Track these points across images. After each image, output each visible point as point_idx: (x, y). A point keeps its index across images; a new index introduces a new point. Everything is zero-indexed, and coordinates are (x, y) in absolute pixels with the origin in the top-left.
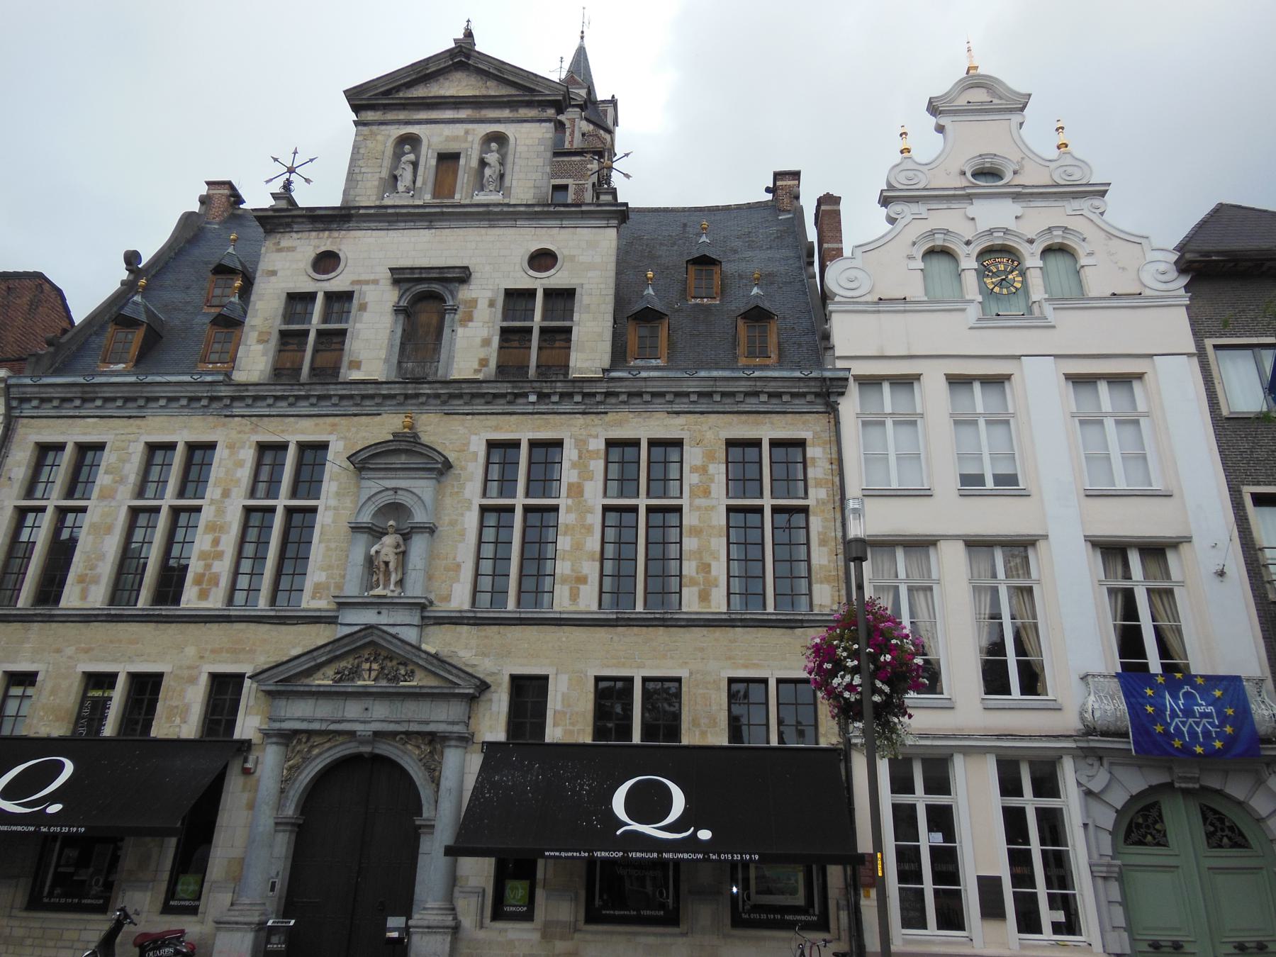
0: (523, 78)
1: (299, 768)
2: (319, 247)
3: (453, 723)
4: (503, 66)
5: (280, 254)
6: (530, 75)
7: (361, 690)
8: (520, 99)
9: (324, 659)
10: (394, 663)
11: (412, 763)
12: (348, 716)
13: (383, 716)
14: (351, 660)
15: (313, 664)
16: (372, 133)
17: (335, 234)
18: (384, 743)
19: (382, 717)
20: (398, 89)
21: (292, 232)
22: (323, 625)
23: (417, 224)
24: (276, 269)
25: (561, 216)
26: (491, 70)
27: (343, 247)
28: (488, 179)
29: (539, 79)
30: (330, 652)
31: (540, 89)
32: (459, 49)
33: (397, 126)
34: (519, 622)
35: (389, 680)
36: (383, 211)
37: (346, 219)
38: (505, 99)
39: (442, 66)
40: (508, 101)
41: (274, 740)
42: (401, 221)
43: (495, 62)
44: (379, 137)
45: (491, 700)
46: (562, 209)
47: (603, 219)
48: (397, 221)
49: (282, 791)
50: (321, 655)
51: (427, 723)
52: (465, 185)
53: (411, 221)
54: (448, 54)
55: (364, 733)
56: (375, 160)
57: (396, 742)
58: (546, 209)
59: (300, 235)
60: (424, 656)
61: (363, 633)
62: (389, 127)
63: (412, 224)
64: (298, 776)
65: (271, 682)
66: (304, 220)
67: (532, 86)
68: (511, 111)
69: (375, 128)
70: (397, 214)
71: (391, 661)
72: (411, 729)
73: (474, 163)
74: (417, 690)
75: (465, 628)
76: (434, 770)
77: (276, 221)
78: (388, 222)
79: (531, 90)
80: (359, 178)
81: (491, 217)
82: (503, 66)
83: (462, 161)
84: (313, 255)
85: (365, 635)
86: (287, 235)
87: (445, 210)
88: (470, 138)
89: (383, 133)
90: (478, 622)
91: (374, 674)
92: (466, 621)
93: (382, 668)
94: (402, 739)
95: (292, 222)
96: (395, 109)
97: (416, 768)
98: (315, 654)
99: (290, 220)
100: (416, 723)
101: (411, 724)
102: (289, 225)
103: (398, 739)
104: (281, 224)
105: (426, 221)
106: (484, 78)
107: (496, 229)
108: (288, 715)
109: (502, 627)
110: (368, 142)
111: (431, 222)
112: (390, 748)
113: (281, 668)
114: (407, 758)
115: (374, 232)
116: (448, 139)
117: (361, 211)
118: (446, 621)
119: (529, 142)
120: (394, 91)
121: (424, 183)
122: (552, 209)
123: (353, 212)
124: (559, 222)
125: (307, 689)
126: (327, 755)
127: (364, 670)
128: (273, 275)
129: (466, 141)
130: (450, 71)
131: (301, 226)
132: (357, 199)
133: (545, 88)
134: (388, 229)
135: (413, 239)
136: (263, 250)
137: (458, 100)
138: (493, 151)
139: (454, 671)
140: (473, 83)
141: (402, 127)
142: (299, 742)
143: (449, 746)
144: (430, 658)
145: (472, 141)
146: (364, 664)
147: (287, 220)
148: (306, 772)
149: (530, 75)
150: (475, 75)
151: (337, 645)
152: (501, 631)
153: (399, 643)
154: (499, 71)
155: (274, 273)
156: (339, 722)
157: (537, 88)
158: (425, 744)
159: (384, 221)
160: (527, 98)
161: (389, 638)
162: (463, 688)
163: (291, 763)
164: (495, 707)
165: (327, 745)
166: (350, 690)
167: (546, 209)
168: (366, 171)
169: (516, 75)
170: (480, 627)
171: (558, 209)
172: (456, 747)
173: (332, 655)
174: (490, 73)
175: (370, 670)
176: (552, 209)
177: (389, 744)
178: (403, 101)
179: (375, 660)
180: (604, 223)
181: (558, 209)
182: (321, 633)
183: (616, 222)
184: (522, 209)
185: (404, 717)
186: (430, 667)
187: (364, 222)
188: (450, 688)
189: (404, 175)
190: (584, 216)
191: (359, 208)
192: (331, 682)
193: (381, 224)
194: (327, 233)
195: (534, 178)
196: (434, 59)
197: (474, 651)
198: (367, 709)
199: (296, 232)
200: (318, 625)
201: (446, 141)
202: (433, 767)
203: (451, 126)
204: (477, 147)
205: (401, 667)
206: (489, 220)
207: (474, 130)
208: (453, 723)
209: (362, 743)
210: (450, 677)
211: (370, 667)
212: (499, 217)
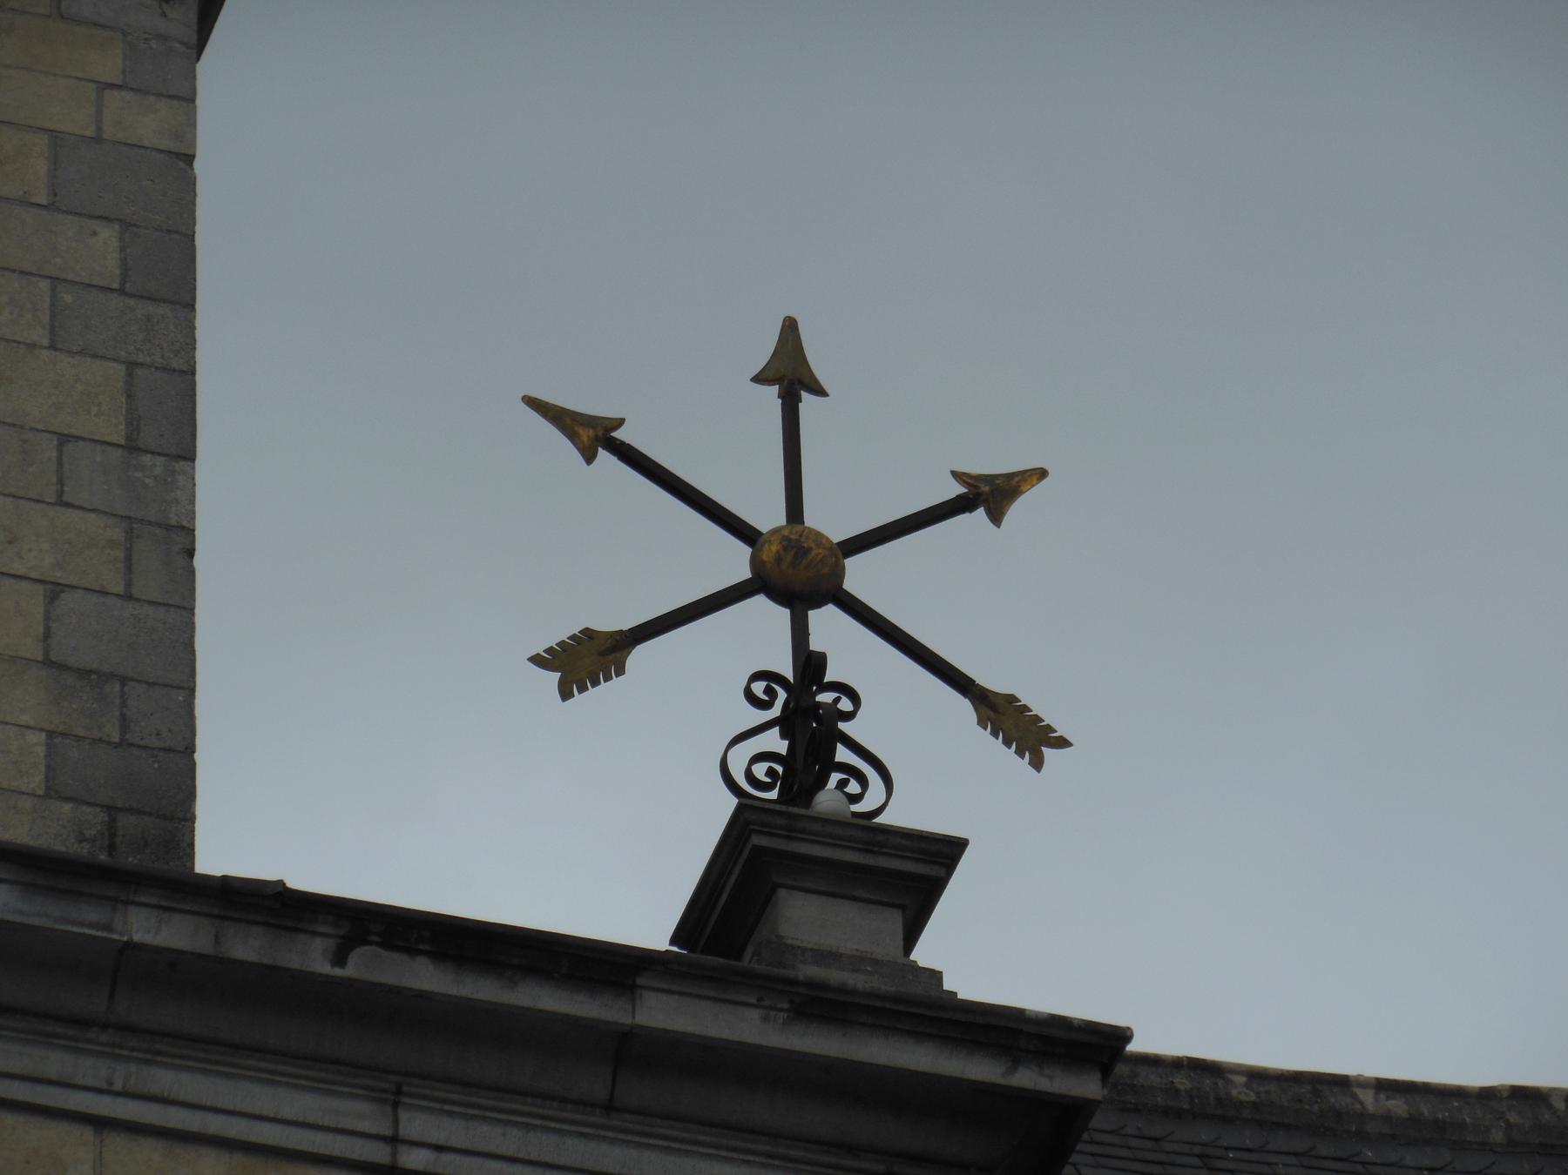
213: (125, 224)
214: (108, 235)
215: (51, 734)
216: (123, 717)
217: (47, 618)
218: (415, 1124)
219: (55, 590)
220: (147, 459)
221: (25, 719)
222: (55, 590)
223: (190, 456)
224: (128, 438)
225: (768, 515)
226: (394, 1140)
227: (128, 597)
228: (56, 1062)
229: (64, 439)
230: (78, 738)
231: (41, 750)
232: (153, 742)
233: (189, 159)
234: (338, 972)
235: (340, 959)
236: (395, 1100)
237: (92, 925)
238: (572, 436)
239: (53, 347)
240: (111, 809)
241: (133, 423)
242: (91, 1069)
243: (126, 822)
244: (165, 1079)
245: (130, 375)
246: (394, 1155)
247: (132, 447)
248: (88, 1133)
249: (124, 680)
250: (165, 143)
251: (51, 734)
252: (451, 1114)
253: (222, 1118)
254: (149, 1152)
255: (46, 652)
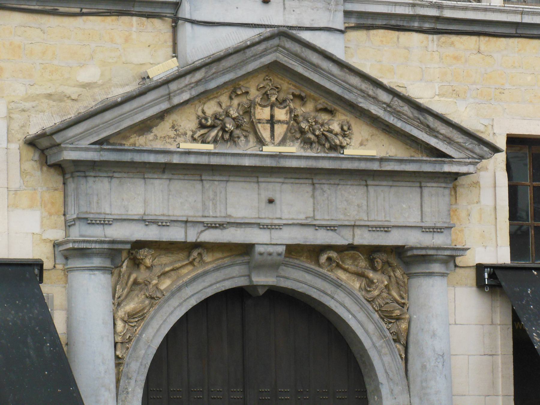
1: (143, 317)
3: (435, 230)
7: (268, 163)
9: (186, 96)
10: (309, 107)
11: (354, 308)
12: (234, 215)
13: (302, 216)
14: (224, 99)
15: (164, 106)
18: (294, 266)
19: (301, 218)
22: (135, 19)
30: (198, 83)
34: (513, 31)
35: (307, 143)
41: (97, 262)
45: (477, 184)
49: (119, 361)
50: (181, 91)
51: (386, 229)
55: (271, 249)
57: (319, 265)
60: (385, 97)
61: (260, 48)
64: (141, 335)
65: (85, 143)
71: (304, 104)
72: (358, 241)
74: (375, 166)
75: (416, 37)
76: (398, 319)
85: (266, 50)
90: (439, 26)
91: (280, 130)
92: (416, 24)
93: (295, 118)
94: (329, 259)
97: (361, 316)
98: (173, 86)
100: (365, 230)
101: (358, 231)
103: (323, 258)
108: (116, 211)
109: (482, 38)
112: (308, 278)
113: (108, 115)
114: (341, 296)
118: (379, 22)
125: (162, 159)
126: (188, 291)
127: (259, 121)
139: (444, 129)
142: (136, 263)
143: (431, 274)
144: (397, 103)
146: (259, 109)
148: (155, 324)
151: (214, 69)
152: (483, 48)
153: (335, 70)
156: (221, 226)
158: (374, 269)
161: (315, 58)
162: (459, 163)
163: (130, 306)
164: (486, 198)
165: (187, 273)
166: (247, 162)
170: (444, 38)
172: (443, 275)
173: (201, 89)
175: (272, 121)
177: (307, 270)
179: (282, 103)
182: (134, 36)
185: (340, 218)
186: (392, 120)
188: (435, 162)
192: (210, 147)
197: (437, 86)
198: (271, 201)
200: (125, 19)
202: (397, 313)
205: (324, 117)
208: (435, 230)
209: (261, 267)
210: (433, 142)
211: (272, 116)
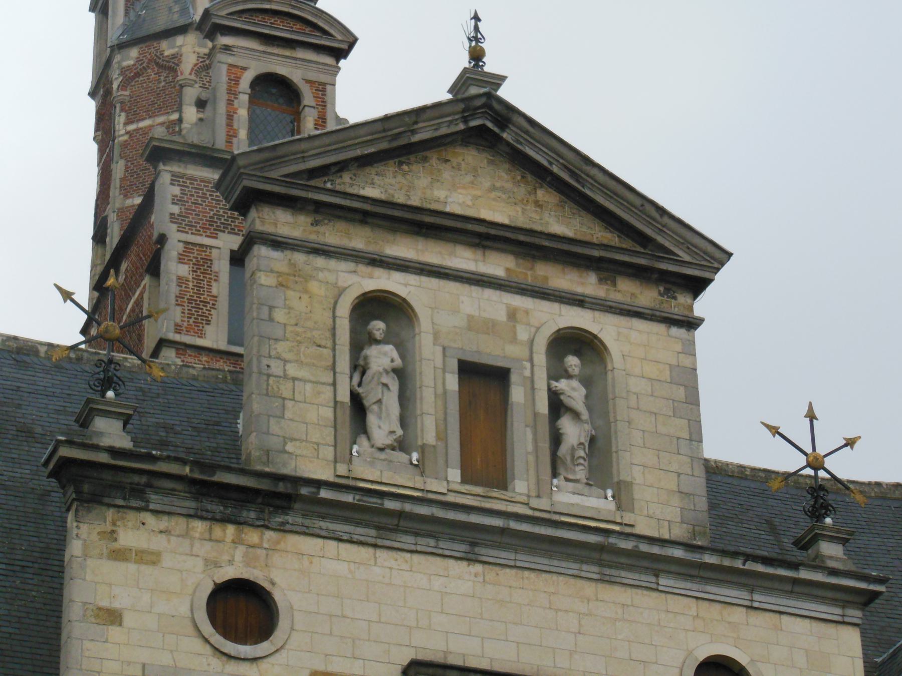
0: (629, 206)
2: (217, 565)
4: (588, 168)
5: (122, 566)
6: (648, 207)
8: (626, 258)
16: (295, 271)
17: (252, 536)
20: (342, 166)
21: (146, 509)
23: (442, 544)
24: (116, 605)
25: (750, 581)
26: (555, 169)
27: (277, 576)
28: (573, 449)
29: (666, 220)
31: (667, 244)
32: (483, 100)
33: (351, 266)
36: (373, 501)
37: (278, 502)
38: (596, 253)
39: (444, 131)
40: (601, 259)
42: (406, 532)
43: (570, 155)
44: (314, 286)
46: (760, 568)
47: (834, 602)
48: (396, 530)
52: (531, 458)
53: (430, 535)
54: (461, 106)
56: (313, 350)
58: (727, 562)
59: (164, 523)
62: (333, 263)
63: (432, 542)
66: (178, 486)
67: (648, 231)
68: (601, 280)
69: (300, 258)
70: (400, 514)
73: (543, 406)
77: (107, 476)
78: (378, 528)
79: (643, 239)
80: (285, 389)
81: (605, 556)
82: (588, 168)
83: (517, 394)
84: (209, 588)
86: (132, 516)
87: (514, 525)
88: (523, 334)
89: (321, 275)
95: (150, 486)
96: (339, 217)
99: (144, 480)
102: (138, 492)
104: (118, 487)
105: (463, 542)
106: (529, 177)
107: (617, 588)
110: (290, 293)
111: (473, 544)
115: (343, 546)
116: (474, 325)
117: (324, 494)
119: (651, 370)
120: (333, 169)
121: (442, 436)
122: (738, 564)
123: (304, 491)
124: (745, 594)
128: (112, 623)
129: (514, 340)
130: (452, 143)
131: (166, 500)
132: (289, 447)
133: (678, 244)
134: (375, 546)
135: (437, 583)
136: (75, 548)
137: (493, 232)
138: (569, 377)
140: (509, 185)
141: (362, 268)
145: (531, 342)
147: (136, 479)
149: (648, 207)
150: (507, 166)
154: (573, 174)
155: (113, 617)
157: (660, 239)
159: (367, 525)
160: (643, 261)
167: (727, 562)
168: (301, 373)
169: (613, 195)
171: (751, 566)
174: (551, 173)
176: (738, 564)
178: (367, 207)
180: (834, 612)
181: (751, 566)
183: (858, 613)
184: (678, 553)
187: (323, 517)
189: (384, 401)
190: (797, 589)
191: (319, 484)
193: (360, 530)
194: (231, 529)
195: (675, 467)
196: (429, 114)
199: (156, 512)
201: (470, 328)
203: (475, 291)
204: (541, 359)
206: (601, 563)
207: (527, 312)
212: (623, 560)
213: (685, 386)
214: (682, 389)
215: (681, 508)
216: (694, 504)
217: (678, 481)
218: (756, 597)
219: (679, 474)
220: (694, 442)
221: (676, 505)
222: (679, 474)
223: (701, 441)
224: (690, 438)
225: (809, 450)
226: (752, 601)
227: (693, 475)
228: (689, 585)
229: (678, 438)
230: (686, 509)
231: (679, 512)
232: (700, 509)
233: (696, 370)
234: (744, 567)
235: (744, 565)
236: (752, 592)
237: (698, 559)
238: (771, 431)
239: (674, 416)
240: (694, 526)
241: (691, 434)
242: (695, 586)
243: (697, 528)
244: (709, 588)
245: (689, 422)
246: (752, 604)
247: (691, 440)
248: (694, 600)
249: (693, 495)
250: (691, 366)
251: (681, 508)
252: (762, 595)
253: (720, 596)
254: (706, 603)
255: (679, 489)
